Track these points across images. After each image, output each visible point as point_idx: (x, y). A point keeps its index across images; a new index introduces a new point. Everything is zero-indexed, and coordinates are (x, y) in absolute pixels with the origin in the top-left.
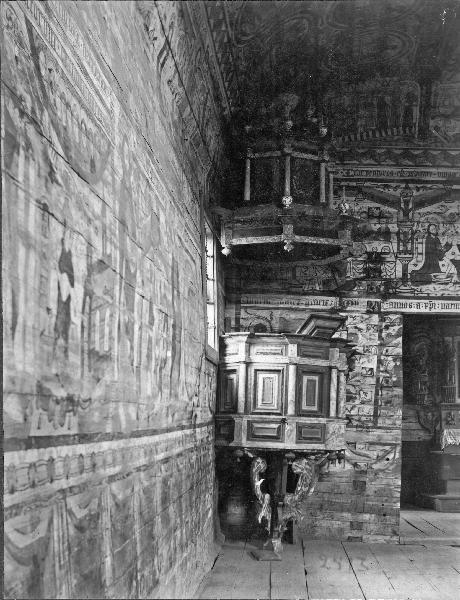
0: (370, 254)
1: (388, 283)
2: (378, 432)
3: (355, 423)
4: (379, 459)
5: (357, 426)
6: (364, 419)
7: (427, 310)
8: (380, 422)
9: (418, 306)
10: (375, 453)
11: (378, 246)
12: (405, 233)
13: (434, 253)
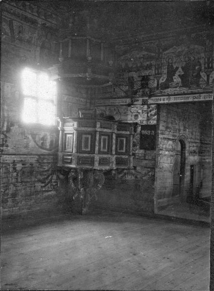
0: (144, 77)
1: (151, 90)
3: (137, 157)
4: (146, 174)
6: (140, 155)
7: (168, 102)
9: (164, 100)
10: (144, 172)
11: (147, 73)
12: (159, 65)
13: (171, 73)
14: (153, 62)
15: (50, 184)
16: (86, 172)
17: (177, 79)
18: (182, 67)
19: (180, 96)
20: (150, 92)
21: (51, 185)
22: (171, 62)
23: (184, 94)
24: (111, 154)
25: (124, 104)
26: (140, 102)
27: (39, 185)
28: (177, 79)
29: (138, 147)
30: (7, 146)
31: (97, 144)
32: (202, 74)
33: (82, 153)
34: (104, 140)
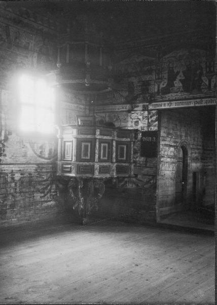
2: (148, 169)
4: (148, 182)
5: (138, 166)
6: (141, 163)
7: (169, 107)
8: (148, 165)
9: (165, 104)
11: (147, 78)
14: (154, 67)
15: (49, 194)
16: (86, 181)
17: (177, 84)
18: (184, 73)
19: (181, 101)
20: (151, 97)
21: (50, 195)
22: (172, 66)
23: (185, 99)
24: (112, 162)
25: (125, 110)
26: (140, 108)
27: (38, 196)
28: (177, 84)
29: (139, 154)
30: (5, 155)
31: (97, 151)
32: (203, 78)
33: (81, 161)
34: (105, 148)
